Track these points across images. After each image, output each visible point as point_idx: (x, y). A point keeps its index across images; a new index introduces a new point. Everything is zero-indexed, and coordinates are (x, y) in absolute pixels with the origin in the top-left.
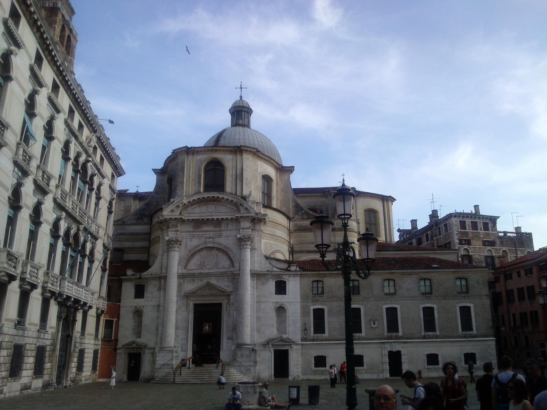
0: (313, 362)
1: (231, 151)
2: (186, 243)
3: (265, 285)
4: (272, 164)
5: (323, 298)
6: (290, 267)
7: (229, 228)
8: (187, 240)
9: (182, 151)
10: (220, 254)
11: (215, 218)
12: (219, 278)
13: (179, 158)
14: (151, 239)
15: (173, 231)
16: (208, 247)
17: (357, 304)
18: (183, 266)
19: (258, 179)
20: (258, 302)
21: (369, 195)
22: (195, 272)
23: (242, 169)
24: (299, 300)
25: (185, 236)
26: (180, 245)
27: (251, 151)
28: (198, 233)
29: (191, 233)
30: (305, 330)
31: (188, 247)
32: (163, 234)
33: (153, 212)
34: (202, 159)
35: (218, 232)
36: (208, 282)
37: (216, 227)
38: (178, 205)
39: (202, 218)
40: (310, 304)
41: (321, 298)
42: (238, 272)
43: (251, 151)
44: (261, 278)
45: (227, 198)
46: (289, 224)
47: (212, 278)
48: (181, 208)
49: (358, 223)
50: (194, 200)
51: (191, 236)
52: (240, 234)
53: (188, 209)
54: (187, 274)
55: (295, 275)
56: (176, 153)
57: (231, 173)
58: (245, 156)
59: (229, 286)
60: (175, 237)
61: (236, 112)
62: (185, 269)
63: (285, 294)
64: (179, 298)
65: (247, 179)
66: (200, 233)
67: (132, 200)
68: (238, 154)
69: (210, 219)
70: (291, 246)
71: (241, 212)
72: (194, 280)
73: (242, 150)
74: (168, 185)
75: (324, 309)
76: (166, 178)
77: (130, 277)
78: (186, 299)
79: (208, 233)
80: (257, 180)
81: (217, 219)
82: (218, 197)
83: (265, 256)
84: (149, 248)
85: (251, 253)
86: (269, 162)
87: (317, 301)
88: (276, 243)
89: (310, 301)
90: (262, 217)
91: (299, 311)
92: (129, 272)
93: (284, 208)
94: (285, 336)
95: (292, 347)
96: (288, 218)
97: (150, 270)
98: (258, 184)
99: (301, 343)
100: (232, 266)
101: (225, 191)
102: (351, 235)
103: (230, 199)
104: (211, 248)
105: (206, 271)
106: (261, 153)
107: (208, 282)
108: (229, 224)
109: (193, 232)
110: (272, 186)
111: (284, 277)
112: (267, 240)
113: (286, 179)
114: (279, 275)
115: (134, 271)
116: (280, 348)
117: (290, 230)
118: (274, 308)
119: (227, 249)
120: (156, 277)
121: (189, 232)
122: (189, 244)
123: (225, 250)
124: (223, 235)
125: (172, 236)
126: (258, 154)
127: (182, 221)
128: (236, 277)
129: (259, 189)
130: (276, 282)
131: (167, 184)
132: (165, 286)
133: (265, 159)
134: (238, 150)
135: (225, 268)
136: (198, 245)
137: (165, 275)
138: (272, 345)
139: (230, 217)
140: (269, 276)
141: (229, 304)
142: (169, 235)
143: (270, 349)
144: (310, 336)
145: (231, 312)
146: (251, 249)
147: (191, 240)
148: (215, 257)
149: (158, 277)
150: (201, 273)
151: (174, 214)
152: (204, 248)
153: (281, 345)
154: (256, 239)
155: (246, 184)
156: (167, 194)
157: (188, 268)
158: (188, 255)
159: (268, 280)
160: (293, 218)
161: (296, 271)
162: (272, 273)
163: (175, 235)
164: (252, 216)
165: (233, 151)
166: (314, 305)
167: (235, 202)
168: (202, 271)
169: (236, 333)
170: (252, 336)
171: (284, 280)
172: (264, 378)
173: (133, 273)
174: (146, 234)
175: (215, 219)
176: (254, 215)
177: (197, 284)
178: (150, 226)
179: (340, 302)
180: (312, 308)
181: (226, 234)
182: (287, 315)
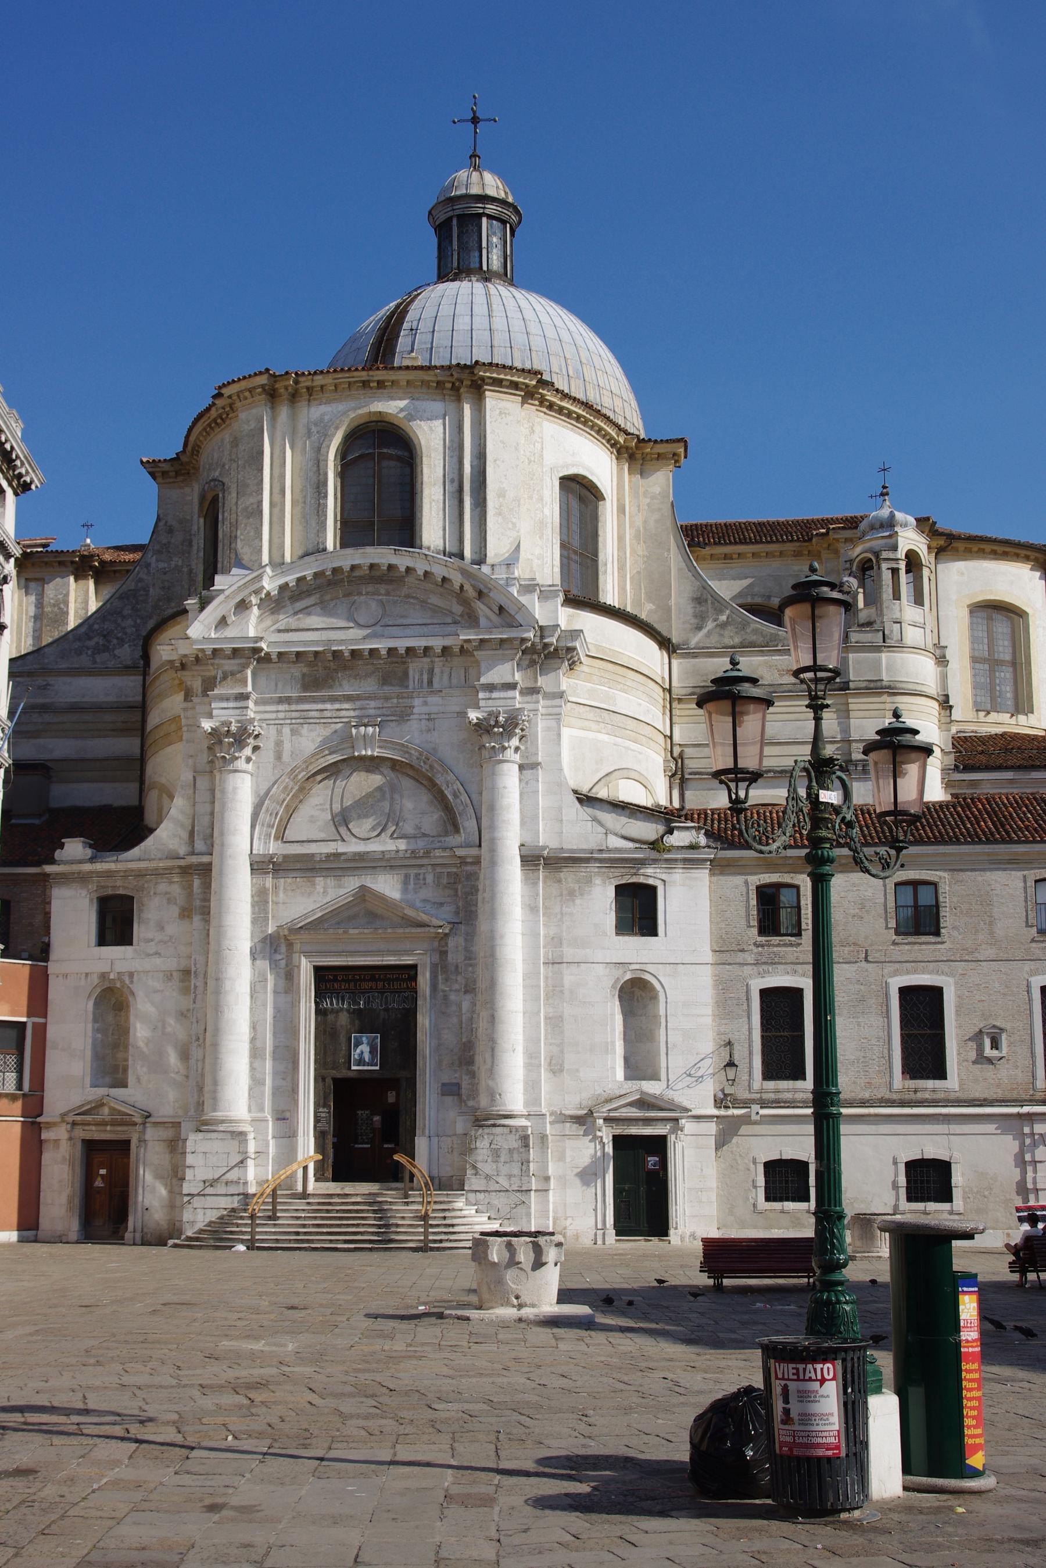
0: (761, 1181)
1: (440, 384)
2: (279, 744)
3: (578, 901)
4: (599, 431)
5: (799, 949)
6: (670, 831)
7: (436, 685)
8: (279, 732)
13: (243, 416)
14: (149, 728)
15: (228, 700)
17: (930, 973)
20: (554, 963)
21: (988, 547)
24: (709, 957)
25: (274, 716)
27: (515, 385)
28: (320, 706)
29: (294, 707)
30: (731, 1064)
31: (286, 757)
32: (194, 708)
33: (151, 624)
34: (326, 418)
35: (395, 701)
36: (363, 887)
37: (385, 681)
38: (243, 601)
40: (748, 970)
42: (474, 851)
43: (515, 385)
44: (562, 875)
46: (667, 667)
48: (255, 609)
49: (942, 660)
51: (294, 714)
52: (477, 707)
54: (285, 857)
55: (690, 863)
56: (230, 397)
58: (494, 402)
59: (442, 904)
60: (238, 721)
61: (455, 222)
65: (502, 494)
66: (328, 706)
67: (72, 579)
70: (677, 751)
71: (483, 621)
73: (483, 379)
74: (202, 520)
75: (802, 990)
76: (192, 494)
77: (75, 868)
78: (283, 949)
80: (541, 499)
82: (391, 567)
83: (575, 792)
84: (142, 761)
85: (520, 780)
86: (585, 423)
88: (619, 740)
89: (750, 958)
90: (562, 644)
92: (74, 848)
93: (650, 606)
94: (652, 1088)
96: (665, 643)
97: (150, 841)
98: (547, 511)
99: (716, 1112)
100: (450, 828)
101: (418, 542)
102: (914, 707)
103: (439, 571)
106: (557, 390)
107: (363, 887)
108: (437, 670)
109: (301, 700)
110: (601, 519)
115: (91, 846)
117: (670, 691)
118: (613, 987)
119: (431, 767)
120: (172, 868)
122: (287, 746)
123: (425, 768)
124: (415, 710)
125: (223, 719)
126: (543, 396)
127: (260, 660)
128: (468, 868)
129: (550, 530)
130: (616, 887)
131: (199, 517)
132: (207, 899)
133: (569, 414)
134: (467, 383)
135: (425, 835)
137: (205, 859)
138: (605, 1120)
141: (445, 969)
142: (215, 712)
145: (453, 997)
146: (521, 767)
147: (294, 732)
148: (388, 796)
149: (180, 867)
150: (337, 855)
151: (229, 632)
154: (541, 726)
156: (201, 554)
157: (290, 835)
159: (589, 881)
160: (686, 643)
161: (693, 847)
163: (238, 712)
165: (449, 385)
167: (457, 586)
168: (342, 848)
169: (473, 1075)
170: (532, 1086)
171: (651, 881)
172: (577, 1237)
173: (89, 852)
174: (131, 707)
175: (384, 652)
176: (531, 635)
177: (325, 892)
178: (141, 678)
179: (864, 964)
180: (759, 983)
181: (425, 709)
182: (662, 1012)
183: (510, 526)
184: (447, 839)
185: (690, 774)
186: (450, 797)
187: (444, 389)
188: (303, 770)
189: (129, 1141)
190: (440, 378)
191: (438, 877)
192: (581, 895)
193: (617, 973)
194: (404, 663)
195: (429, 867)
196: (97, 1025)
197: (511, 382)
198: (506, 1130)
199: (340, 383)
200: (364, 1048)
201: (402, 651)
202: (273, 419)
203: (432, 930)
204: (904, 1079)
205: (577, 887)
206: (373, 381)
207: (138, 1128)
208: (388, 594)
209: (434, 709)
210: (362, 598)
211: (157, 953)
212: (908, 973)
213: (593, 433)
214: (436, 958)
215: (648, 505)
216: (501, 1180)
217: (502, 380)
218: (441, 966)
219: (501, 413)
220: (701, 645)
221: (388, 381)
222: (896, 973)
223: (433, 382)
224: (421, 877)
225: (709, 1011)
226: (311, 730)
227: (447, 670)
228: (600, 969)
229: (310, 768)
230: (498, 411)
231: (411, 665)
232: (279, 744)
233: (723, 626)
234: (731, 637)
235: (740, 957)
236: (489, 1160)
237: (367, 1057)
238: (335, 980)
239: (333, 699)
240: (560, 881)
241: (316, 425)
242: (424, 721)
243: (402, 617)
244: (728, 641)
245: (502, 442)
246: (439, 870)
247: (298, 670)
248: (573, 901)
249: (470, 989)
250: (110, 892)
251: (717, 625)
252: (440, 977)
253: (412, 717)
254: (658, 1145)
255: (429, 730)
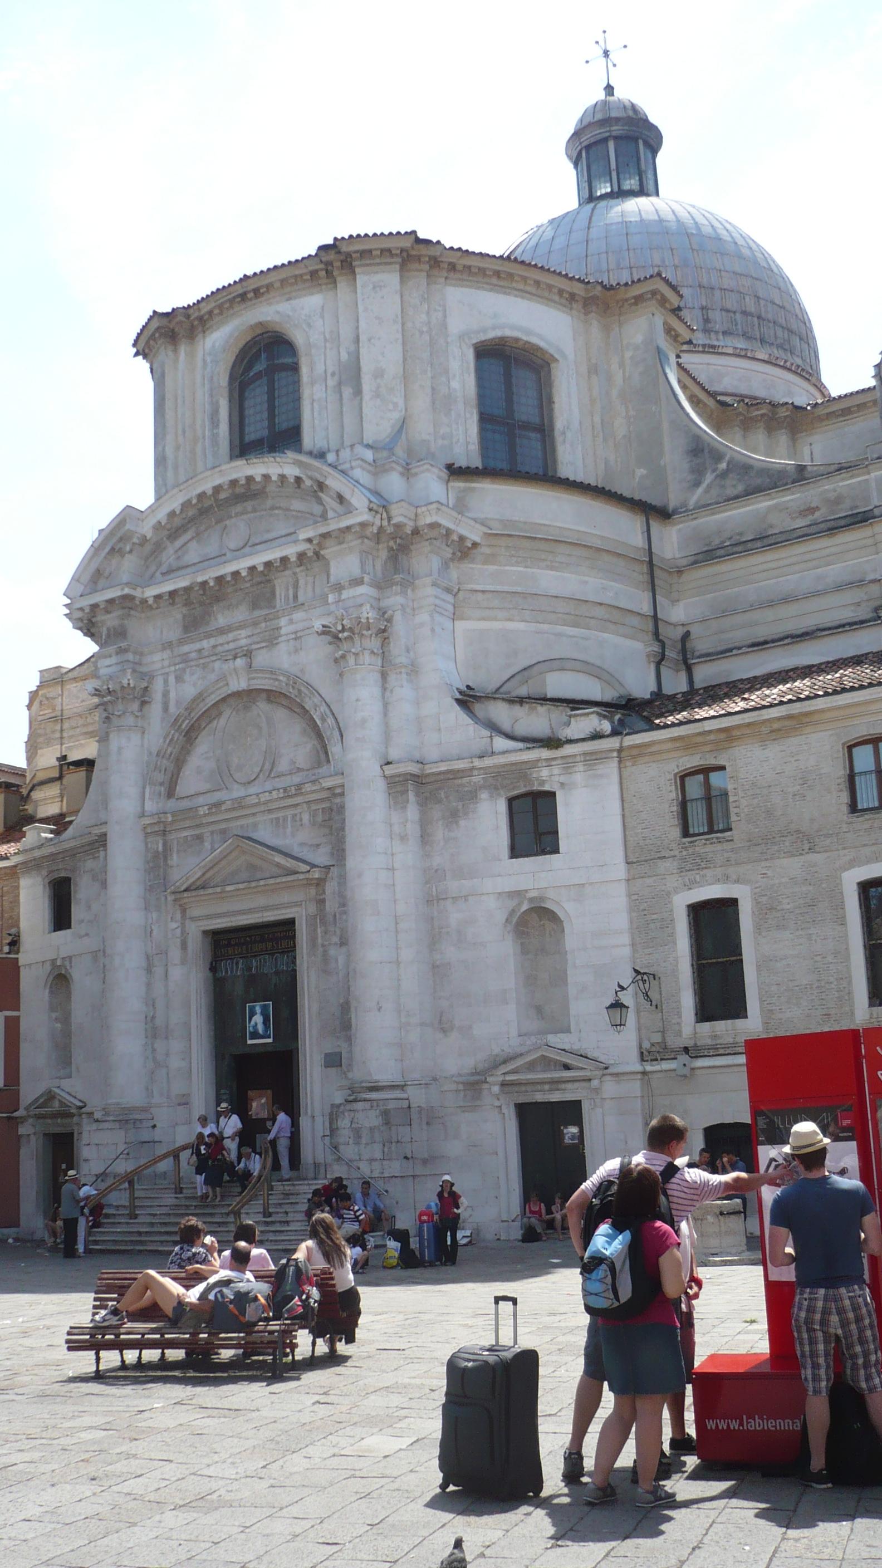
1: (314, 274)
2: (166, 694)
3: (462, 823)
7: (301, 599)
8: (166, 681)
9: (152, 337)
10: (280, 715)
11: (242, 565)
12: (280, 814)
16: (237, 694)
18: (161, 784)
19: (455, 365)
22: (201, 800)
23: (357, 340)
24: (619, 870)
26: (143, 703)
28: (198, 646)
31: (172, 709)
34: (217, 344)
35: (263, 625)
37: (255, 606)
38: (113, 549)
39: (200, 579)
41: (719, 847)
45: (279, 471)
47: (259, 818)
50: (172, 514)
51: (178, 660)
53: (164, 556)
55: (592, 759)
57: (323, 367)
59: (318, 845)
62: (170, 794)
63: (556, 851)
64: (155, 915)
65: (379, 374)
68: (338, 279)
69: (229, 578)
72: (199, 838)
73: (349, 255)
78: (178, 916)
79: (231, 636)
81: (252, 569)
82: (250, 479)
85: (384, 689)
87: (701, 864)
91: (621, 920)
93: (641, 472)
95: (597, 1090)
99: (639, 1068)
100: (323, 756)
104: (247, 696)
105: (238, 792)
108: (301, 582)
109: (181, 642)
111: (545, 773)
112: (483, 619)
113: (639, 339)
114: (521, 770)
116: (539, 1097)
121: (168, 645)
122: (172, 695)
123: (293, 693)
124: (283, 631)
128: (338, 800)
130: (511, 801)
134: (338, 264)
135: (299, 770)
136: (200, 694)
138: (503, 1084)
139: (291, 551)
140: (477, 779)
141: (323, 921)
143: (497, 1103)
144: (679, 1033)
145: (332, 952)
147: (179, 679)
150: (218, 805)
152: (224, 700)
153: (542, 1083)
155: (377, 395)
157: (181, 790)
158: (172, 740)
159: (472, 796)
160: (684, 505)
161: (597, 736)
162: (488, 762)
164: (363, 525)
165: (323, 273)
166: (689, 887)
171: (547, 788)
179: (811, 857)
180: (682, 900)
181: (292, 628)
183: (391, 407)
184: (320, 770)
185: (699, 657)
186: (319, 722)
187: (319, 278)
188: (186, 718)
189: (73, 1134)
190: (310, 268)
191: (314, 814)
192: (466, 814)
193: (511, 904)
194: (269, 581)
195: (305, 805)
196: (54, 1015)
197: (382, 251)
198: (367, 1105)
199: (222, 304)
200: (258, 1019)
201: (261, 568)
202: (176, 360)
203: (301, 876)
204: (871, 1005)
205: (460, 807)
206: (249, 292)
207: (75, 1119)
208: (254, 510)
209: (300, 626)
210: (233, 520)
211: (87, 935)
212: (868, 861)
213: (528, 288)
214: (312, 909)
215: (632, 358)
216: (361, 1165)
217: (370, 251)
218: (320, 917)
219: (374, 288)
220: (702, 502)
221: (262, 287)
222: (852, 864)
223: (305, 274)
224: (298, 818)
225: (626, 939)
226: (193, 674)
227: (310, 579)
228: (491, 903)
229: (192, 715)
230: (371, 286)
231: (276, 582)
232: (166, 694)
233: (724, 475)
234: (734, 486)
235: (663, 866)
236: (351, 1141)
237: (260, 1029)
238: (229, 945)
239: (208, 636)
240: (440, 801)
241: (210, 354)
242: (292, 642)
243: (268, 531)
244: (730, 492)
245: (377, 318)
246: (314, 807)
247: (178, 613)
248: (457, 823)
249: (344, 942)
250: (56, 875)
251: (717, 477)
252: (319, 930)
253: (280, 639)
254: (572, 1111)
255: (296, 651)
